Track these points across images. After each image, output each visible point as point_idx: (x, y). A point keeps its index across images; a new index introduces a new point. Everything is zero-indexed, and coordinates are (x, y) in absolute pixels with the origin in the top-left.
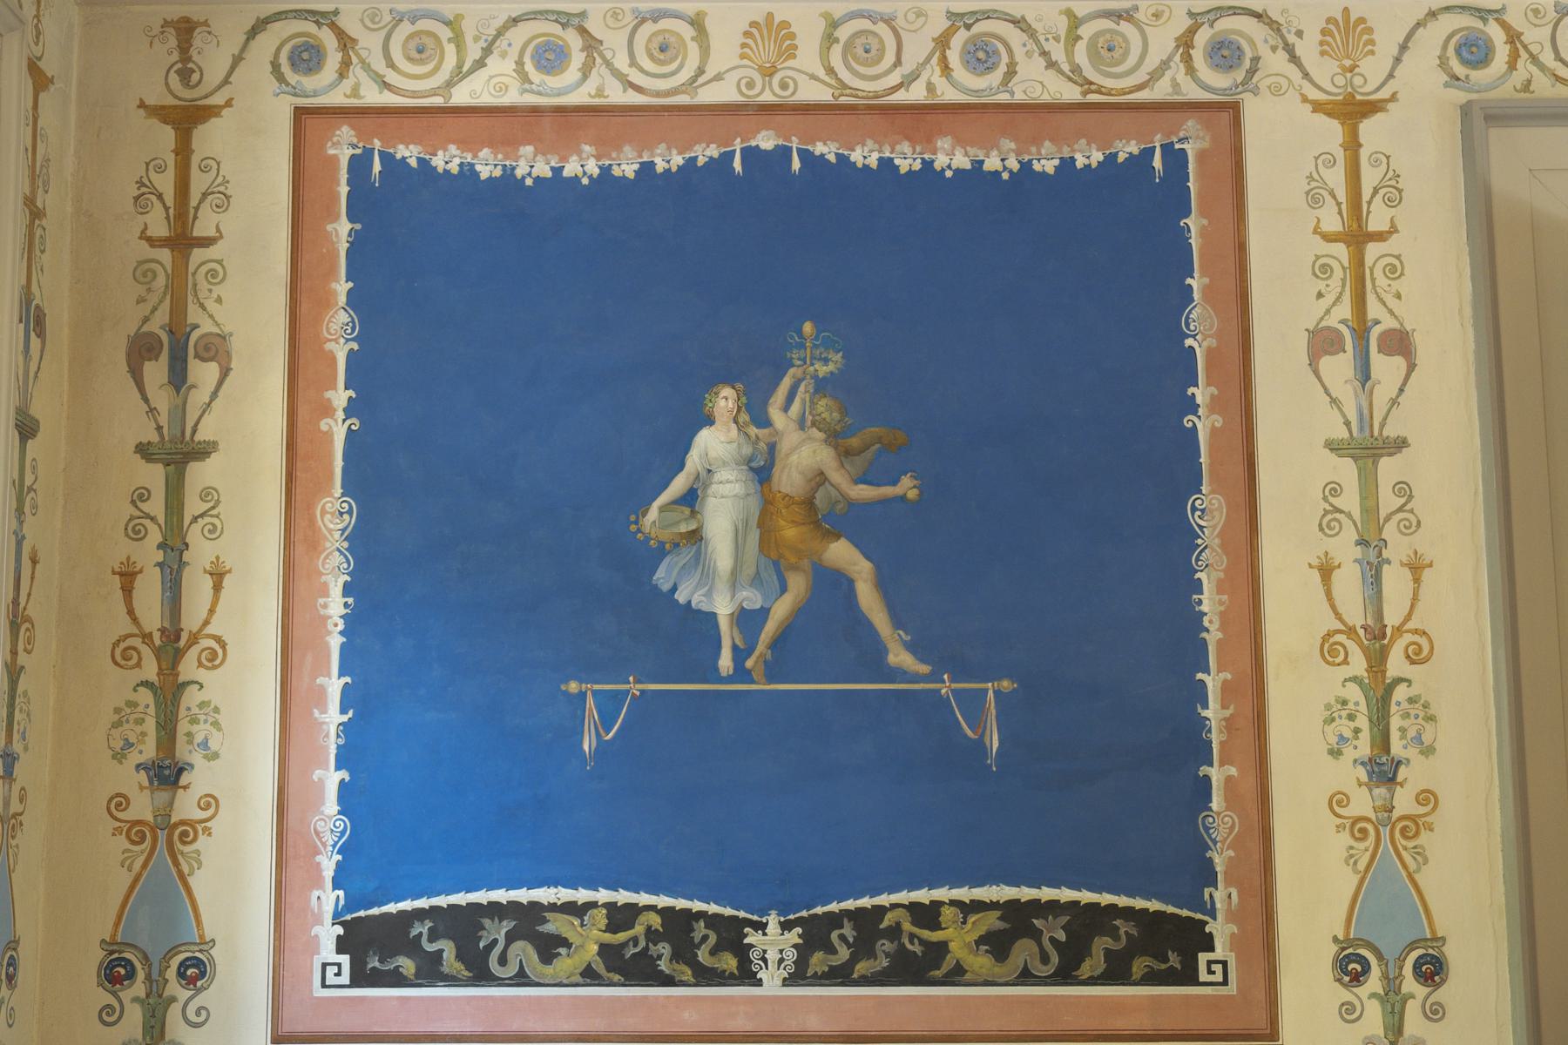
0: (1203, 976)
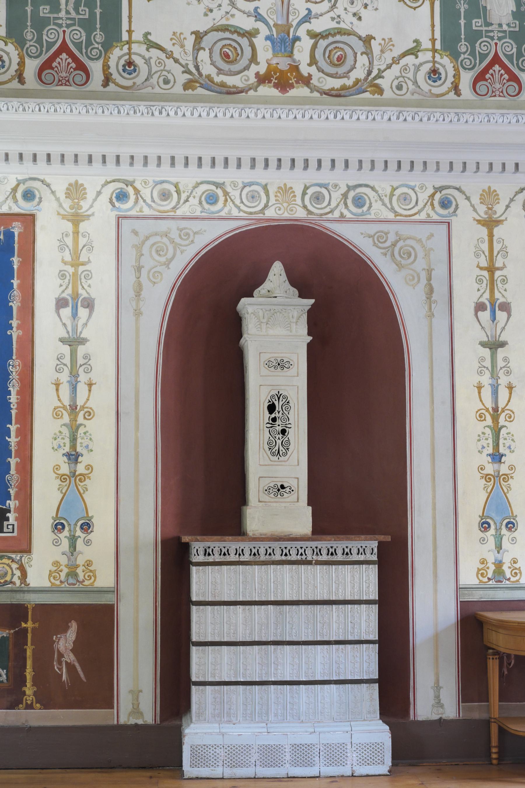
0: (5, 530)
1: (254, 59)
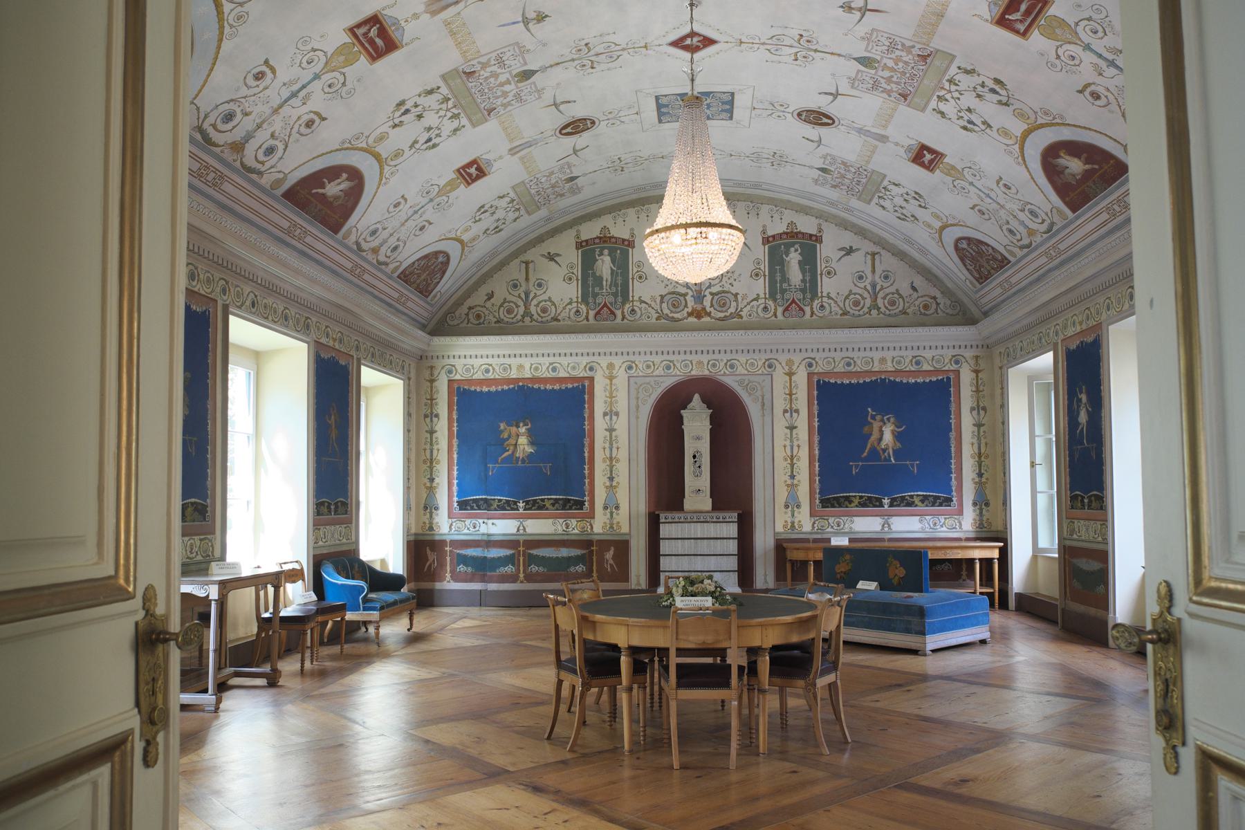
1: (686, 306)
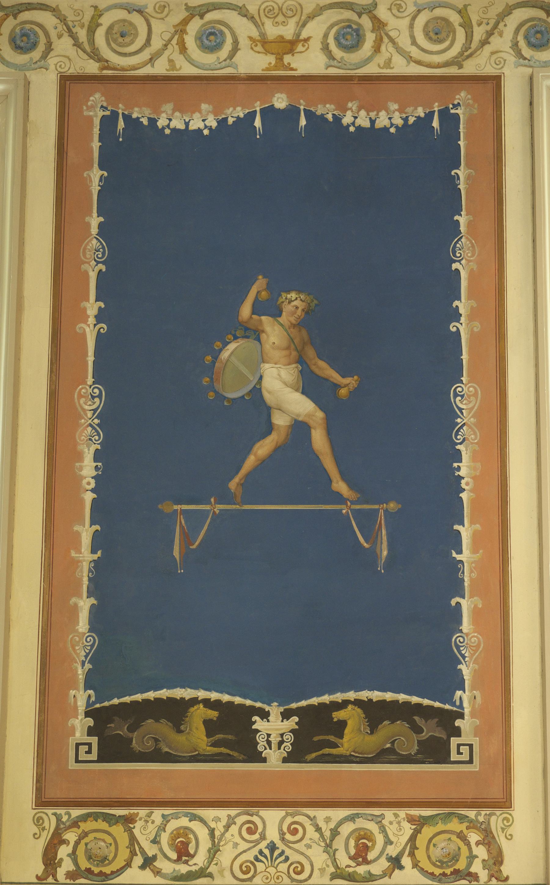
0: (454, 756)
